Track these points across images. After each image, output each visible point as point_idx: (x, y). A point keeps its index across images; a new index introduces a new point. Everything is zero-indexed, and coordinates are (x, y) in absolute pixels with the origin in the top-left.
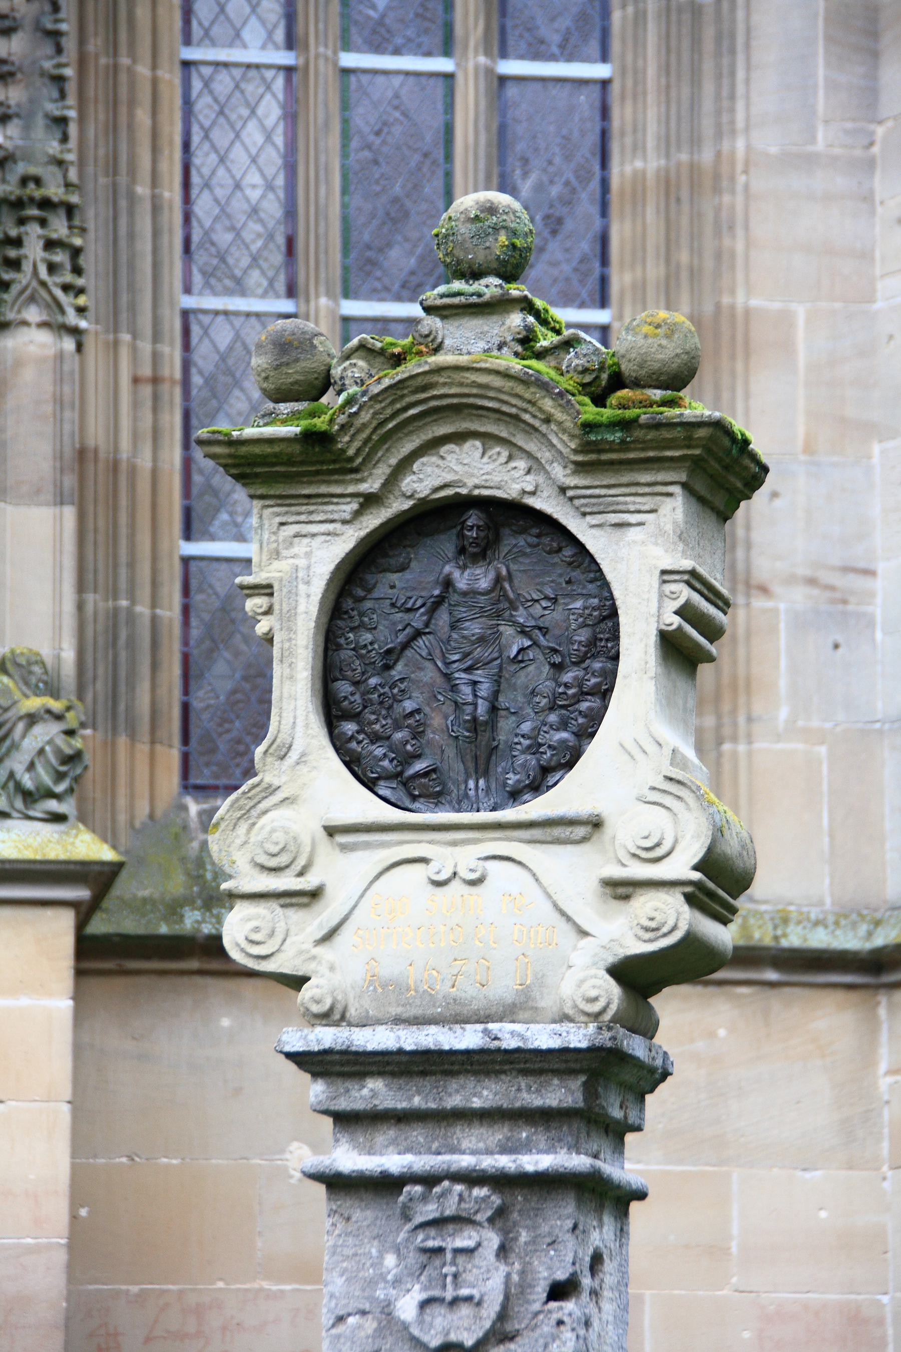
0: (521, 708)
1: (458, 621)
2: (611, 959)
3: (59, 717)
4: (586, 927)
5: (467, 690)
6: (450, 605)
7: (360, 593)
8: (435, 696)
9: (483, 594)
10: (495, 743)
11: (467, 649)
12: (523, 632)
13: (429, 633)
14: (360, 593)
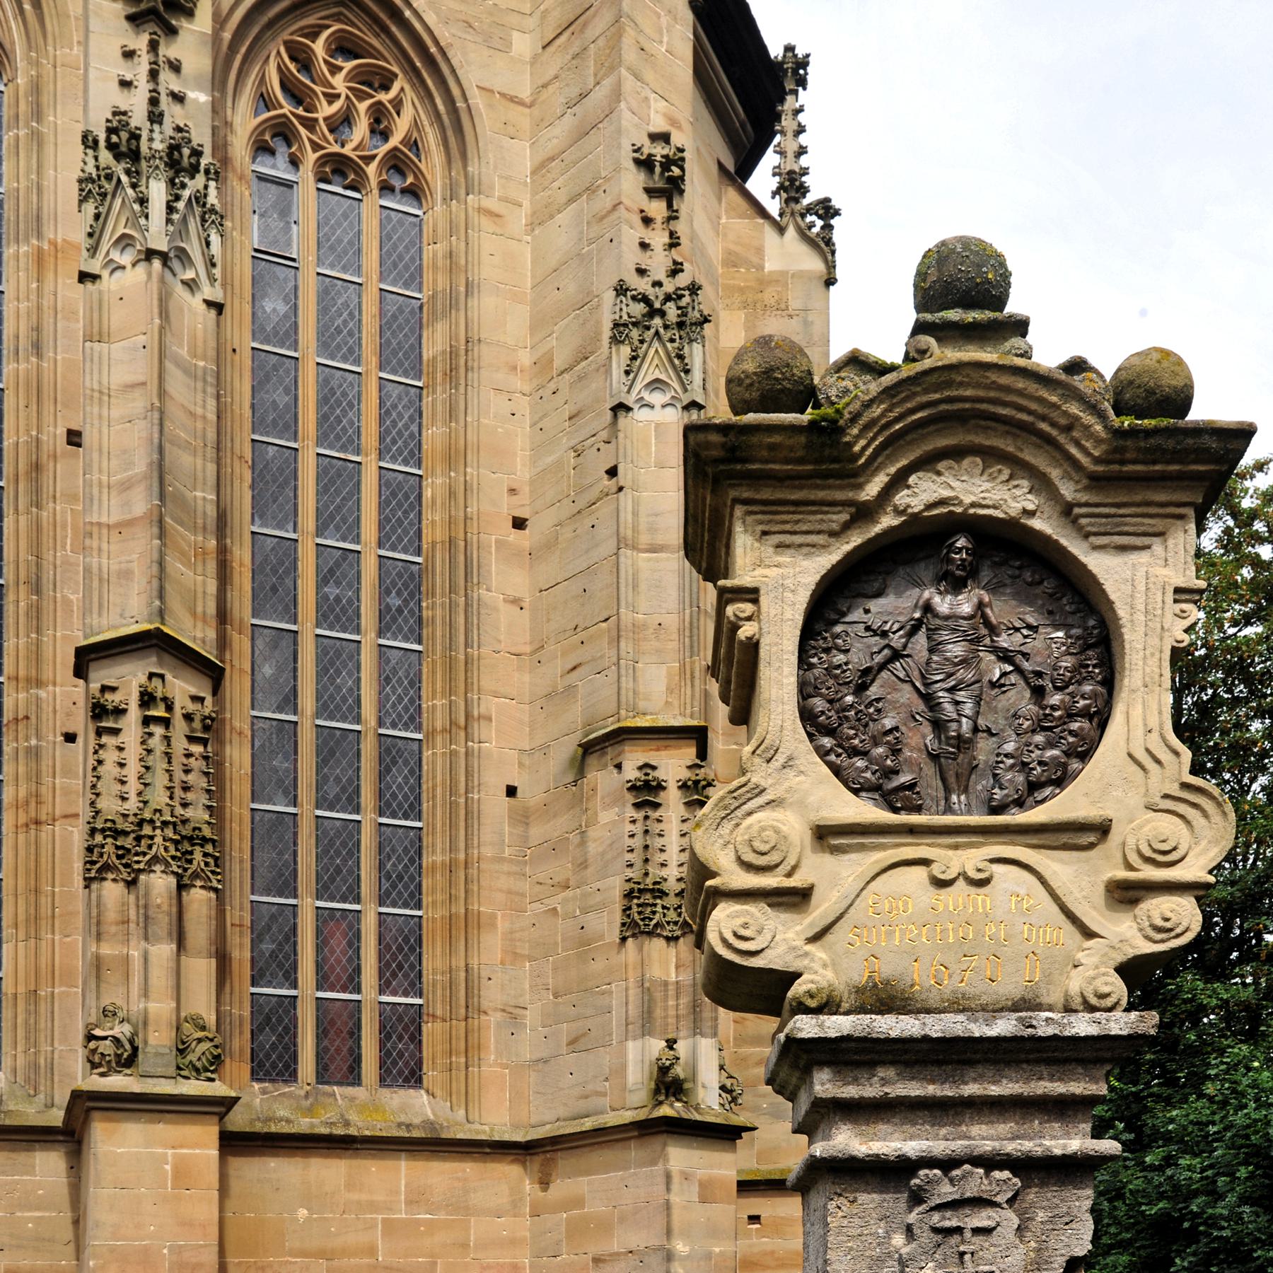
0: (1002, 730)
1: (940, 643)
2: (1120, 958)
3: (211, 1040)
4: (1094, 927)
5: (949, 708)
6: (928, 629)
7: (833, 616)
8: (913, 717)
9: (964, 618)
10: (975, 763)
11: (952, 670)
12: (1005, 656)
13: (908, 656)
14: (833, 616)
